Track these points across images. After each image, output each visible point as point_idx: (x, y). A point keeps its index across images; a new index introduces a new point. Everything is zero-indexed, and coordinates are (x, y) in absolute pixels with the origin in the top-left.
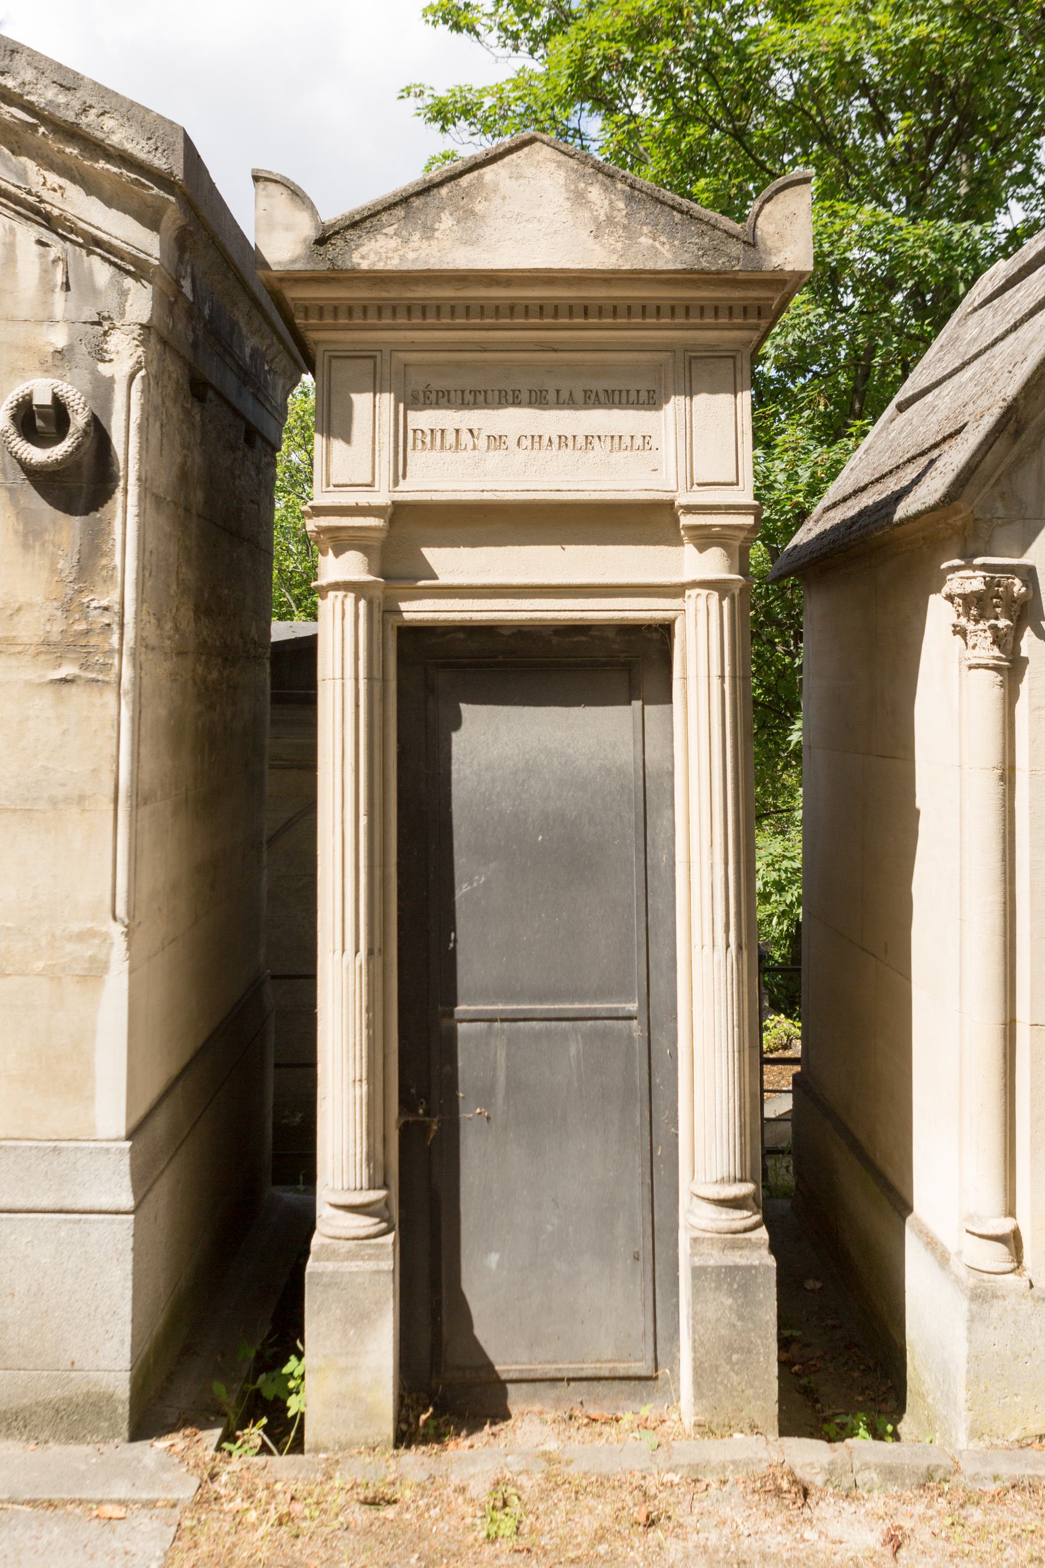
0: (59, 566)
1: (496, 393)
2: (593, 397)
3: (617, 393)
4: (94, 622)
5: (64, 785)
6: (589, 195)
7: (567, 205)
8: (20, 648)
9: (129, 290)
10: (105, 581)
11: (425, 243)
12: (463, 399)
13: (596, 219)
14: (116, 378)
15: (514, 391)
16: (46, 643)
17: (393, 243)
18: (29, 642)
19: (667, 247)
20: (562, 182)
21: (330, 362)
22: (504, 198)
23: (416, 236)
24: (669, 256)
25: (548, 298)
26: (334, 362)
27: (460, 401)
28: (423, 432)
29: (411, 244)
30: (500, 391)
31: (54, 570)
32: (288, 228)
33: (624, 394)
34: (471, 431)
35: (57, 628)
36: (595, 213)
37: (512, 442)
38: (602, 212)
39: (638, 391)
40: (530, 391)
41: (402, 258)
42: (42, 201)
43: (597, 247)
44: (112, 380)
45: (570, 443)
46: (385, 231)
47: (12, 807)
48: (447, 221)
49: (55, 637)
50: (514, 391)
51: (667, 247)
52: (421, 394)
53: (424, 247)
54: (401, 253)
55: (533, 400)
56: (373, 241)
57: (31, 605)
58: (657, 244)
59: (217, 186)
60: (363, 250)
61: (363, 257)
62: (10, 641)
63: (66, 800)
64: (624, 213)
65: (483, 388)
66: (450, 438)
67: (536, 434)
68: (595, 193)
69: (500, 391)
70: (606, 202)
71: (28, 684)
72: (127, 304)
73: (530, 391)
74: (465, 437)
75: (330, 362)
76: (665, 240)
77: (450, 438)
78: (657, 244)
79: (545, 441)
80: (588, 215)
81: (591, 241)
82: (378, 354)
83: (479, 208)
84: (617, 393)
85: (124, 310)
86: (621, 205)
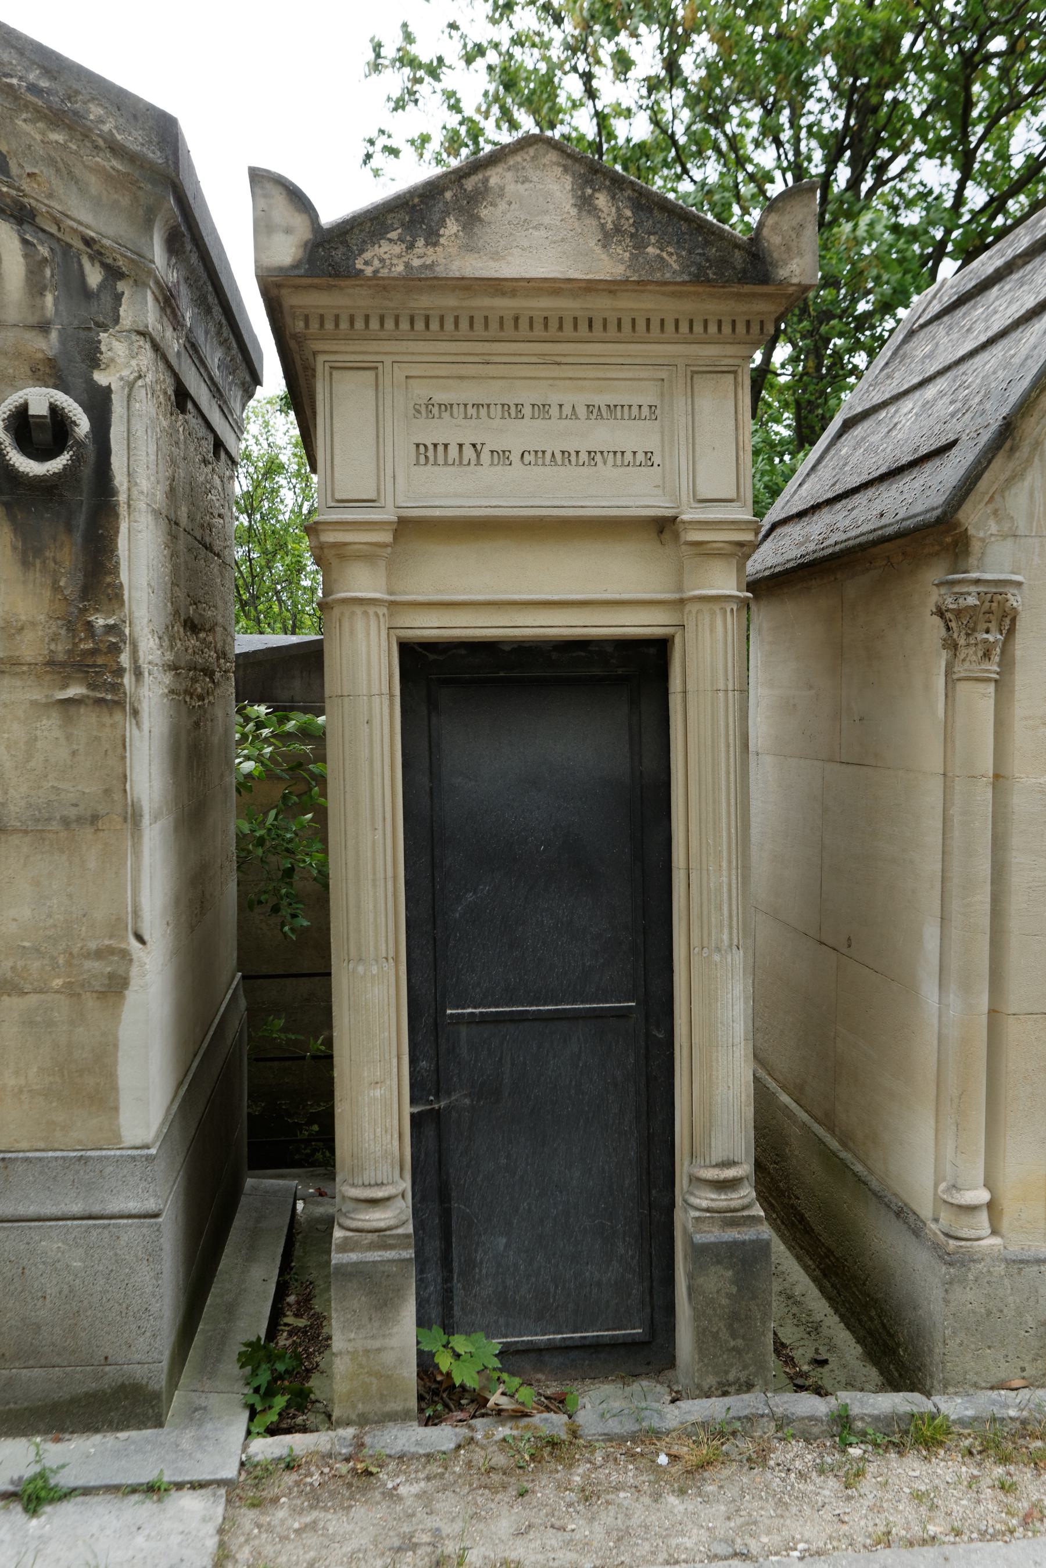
0: (62, 584)
1: (499, 407)
2: (595, 411)
3: (619, 408)
4: (101, 641)
5: (76, 805)
6: (597, 202)
7: (574, 211)
8: (25, 668)
9: (123, 293)
10: (110, 600)
11: (430, 250)
12: (466, 413)
13: (603, 226)
14: (113, 387)
15: (517, 405)
16: (51, 663)
17: (397, 249)
18: (33, 661)
19: (675, 257)
20: (570, 187)
21: (331, 374)
22: (510, 203)
23: (420, 242)
24: (676, 266)
25: (567, 309)
26: (335, 373)
27: (463, 416)
28: (425, 446)
29: (416, 251)
30: (503, 405)
31: (56, 588)
32: (288, 231)
33: (626, 409)
34: (474, 445)
35: (61, 648)
36: (603, 221)
37: (515, 457)
38: (609, 220)
39: (640, 406)
40: (533, 405)
41: (407, 265)
42: (25, 196)
43: (604, 257)
44: (108, 390)
45: (573, 458)
46: (389, 236)
47: (24, 828)
48: (452, 227)
49: (61, 657)
50: (517, 405)
51: (675, 257)
52: (423, 406)
53: (429, 253)
54: (405, 259)
55: (536, 415)
56: (376, 246)
57: (33, 624)
58: (664, 254)
59: (201, 184)
60: (367, 255)
61: (366, 263)
62: (15, 662)
63: (79, 820)
64: (631, 221)
65: (486, 401)
66: (453, 451)
67: (619, 450)
68: (602, 200)
69: (503, 405)
70: (614, 210)
71: (34, 703)
72: (121, 309)
73: (533, 405)
74: (469, 453)
75: (331, 374)
76: (673, 251)
77: (453, 451)
78: (664, 254)
79: (548, 455)
80: (595, 223)
81: (598, 250)
82: (380, 365)
83: (484, 213)
84: (619, 408)
85: (119, 316)
86: (628, 213)
